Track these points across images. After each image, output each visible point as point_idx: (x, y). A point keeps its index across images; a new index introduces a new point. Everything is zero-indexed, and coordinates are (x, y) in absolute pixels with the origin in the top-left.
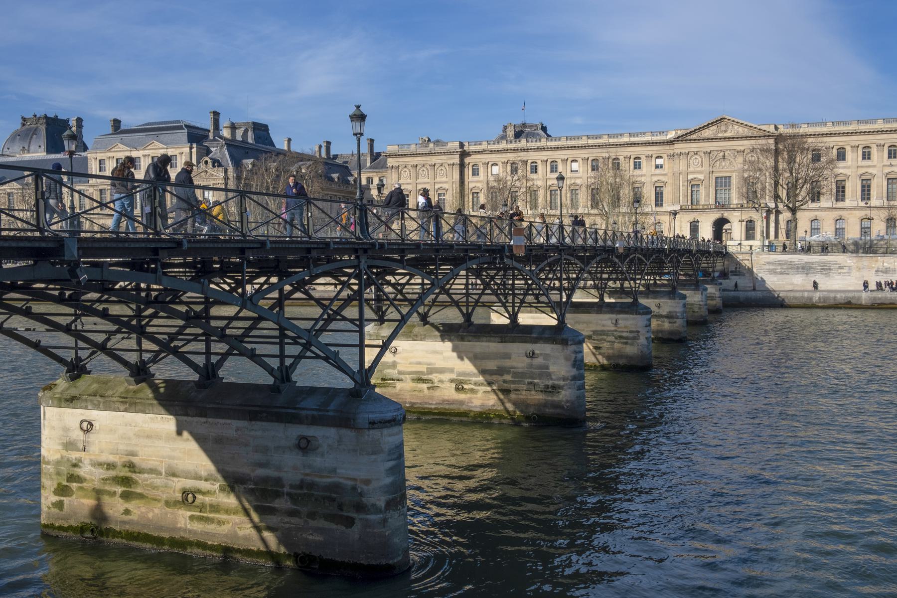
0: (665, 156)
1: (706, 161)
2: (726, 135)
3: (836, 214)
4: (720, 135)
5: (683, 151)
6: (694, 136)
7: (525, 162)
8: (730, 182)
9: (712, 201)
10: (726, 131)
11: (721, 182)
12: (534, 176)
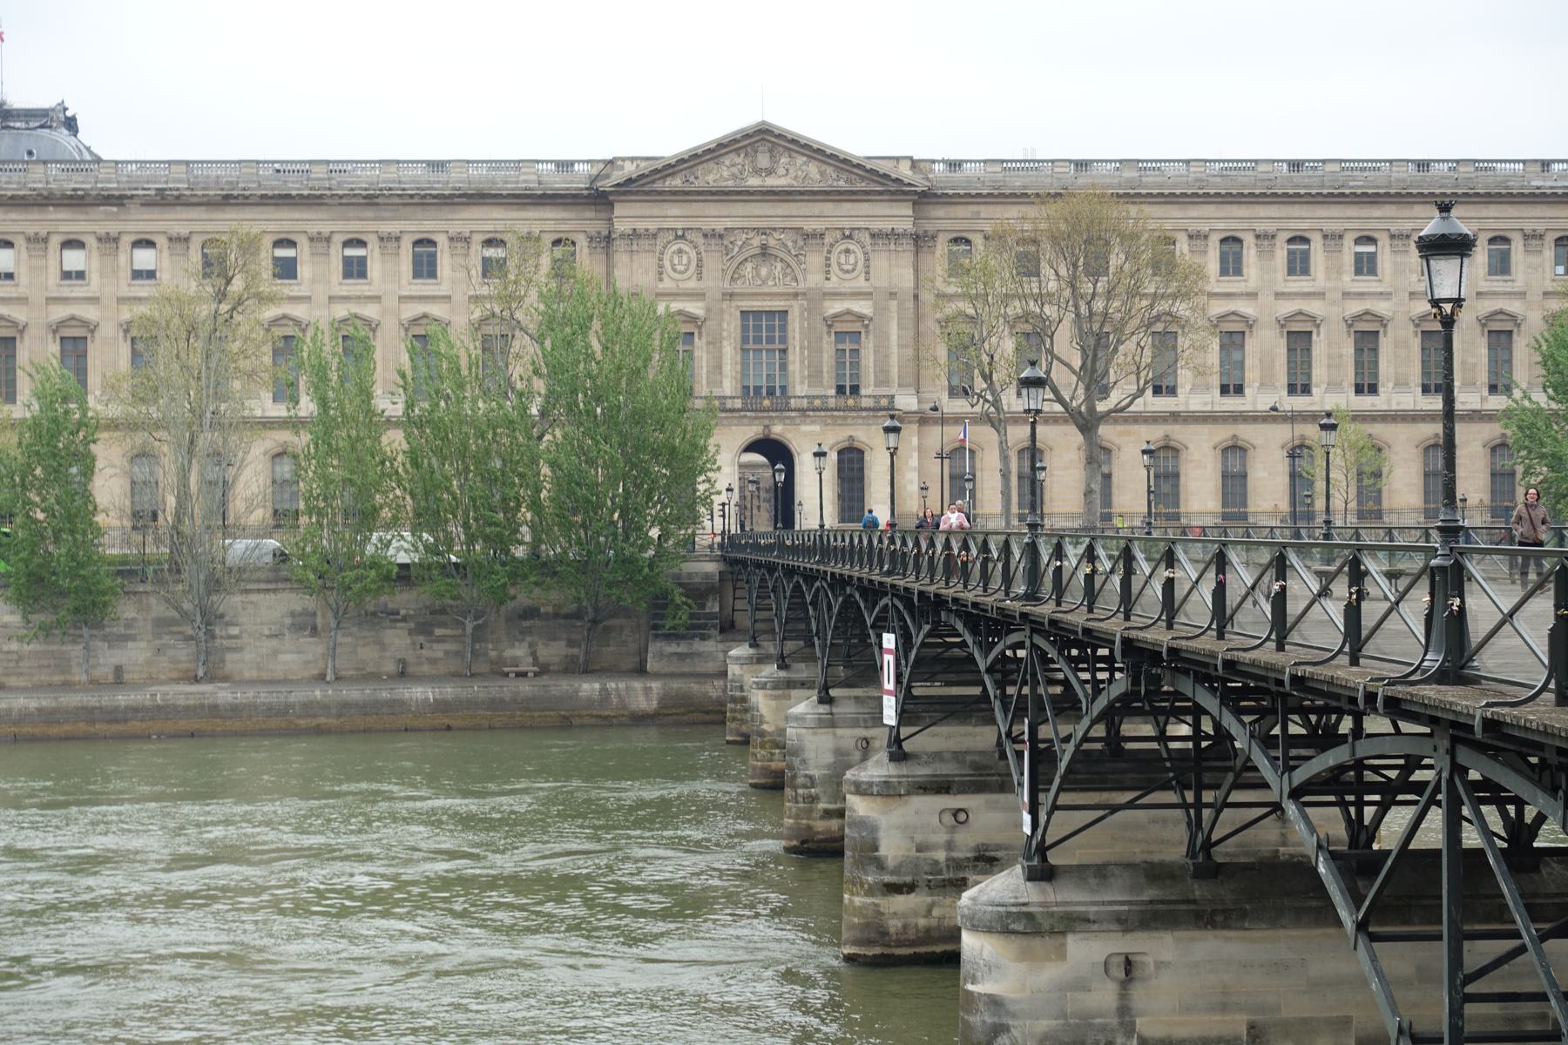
0: (582, 241)
1: (713, 262)
2: (772, 182)
3: (1223, 433)
4: (754, 182)
5: (641, 225)
6: (676, 183)
7: (249, 246)
8: (783, 328)
9: (729, 387)
10: (770, 172)
11: (758, 328)
12: (287, 288)
